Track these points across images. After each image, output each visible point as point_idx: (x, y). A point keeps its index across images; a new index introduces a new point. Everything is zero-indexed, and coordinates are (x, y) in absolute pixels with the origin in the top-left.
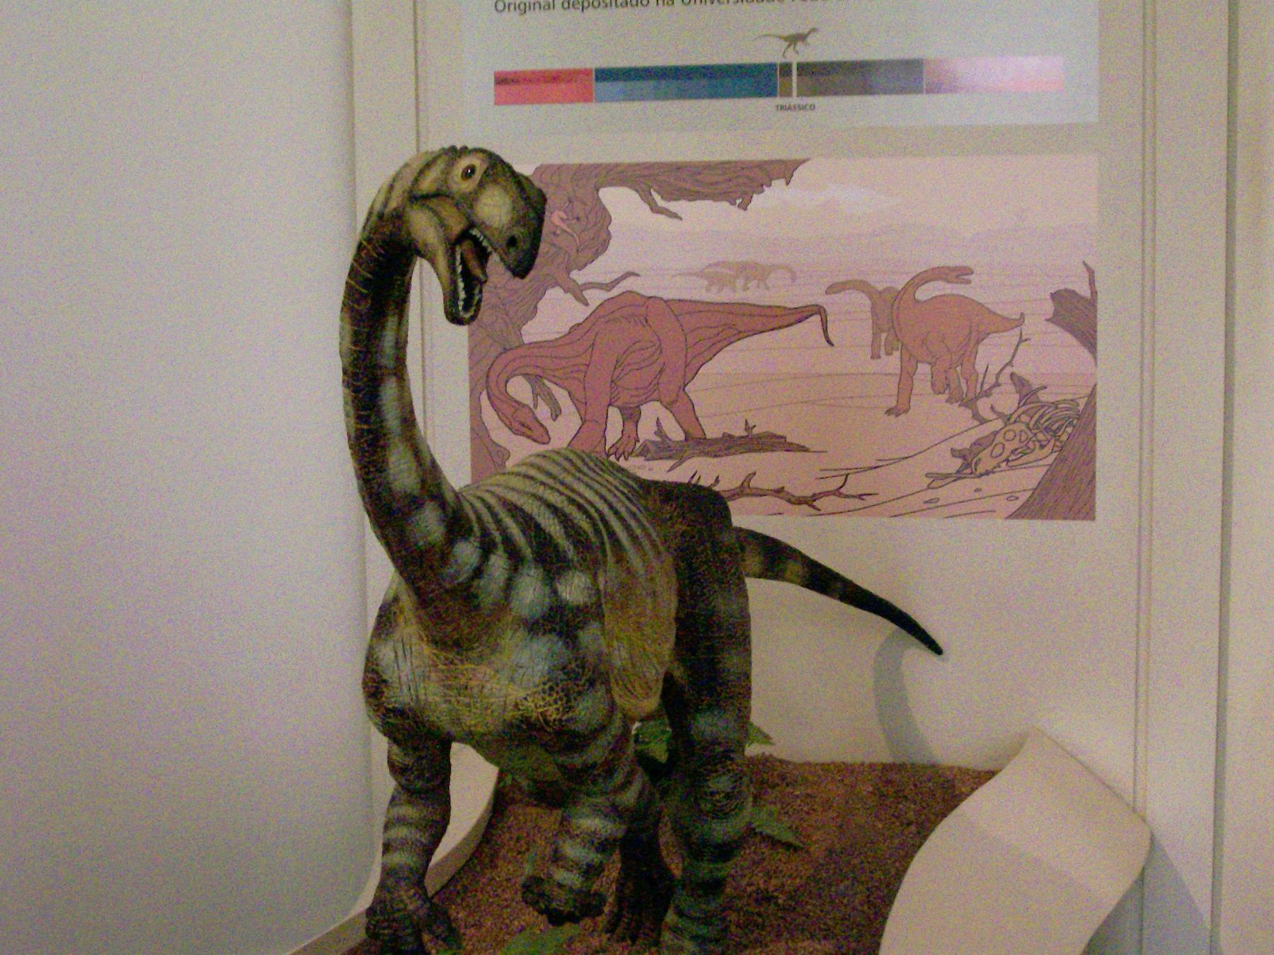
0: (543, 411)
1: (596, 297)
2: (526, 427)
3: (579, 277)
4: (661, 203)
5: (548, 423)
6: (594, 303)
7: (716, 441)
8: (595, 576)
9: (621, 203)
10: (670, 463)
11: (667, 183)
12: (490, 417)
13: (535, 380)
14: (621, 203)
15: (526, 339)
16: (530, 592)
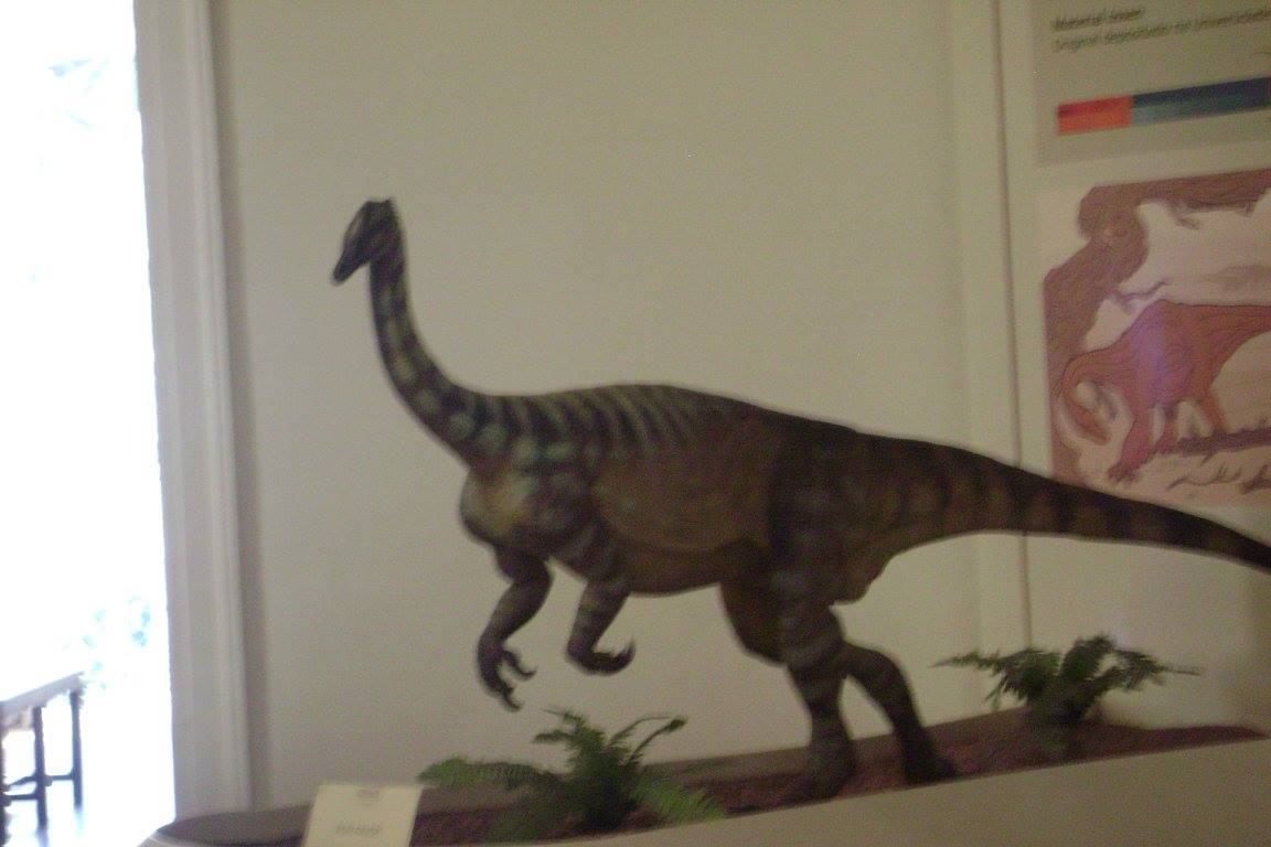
0: (1102, 413)
1: (1140, 305)
2: (1092, 429)
3: (1130, 285)
4: (1186, 216)
6: (1138, 311)
7: (1235, 435)
9: (1153, 214)
10: (1202, 458)
11: (1194, 194)
12: (1065, 423)
13: (1097, 382)
14: (1153, 214)
16: (525, 450)
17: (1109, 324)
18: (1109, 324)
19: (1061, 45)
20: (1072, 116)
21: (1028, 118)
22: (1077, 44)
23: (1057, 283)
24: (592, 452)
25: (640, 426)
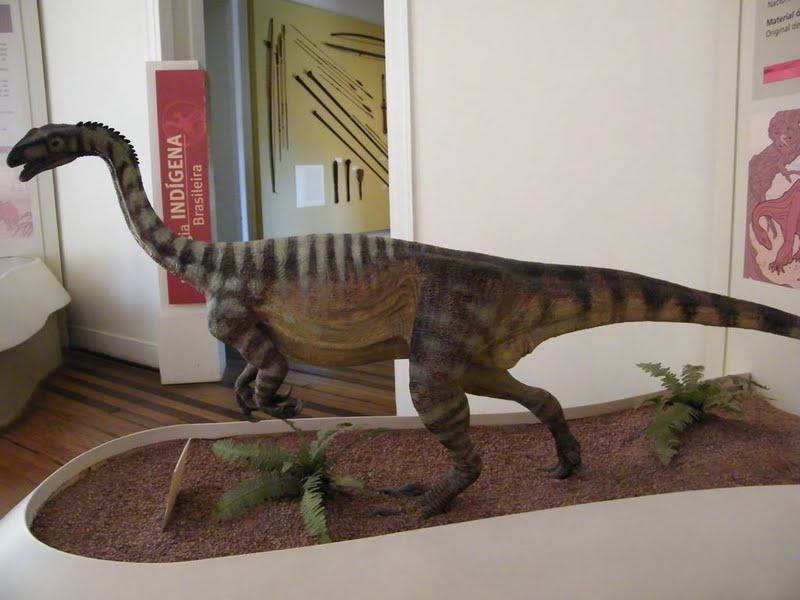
0: (770, 234)
1: (794, 178)
2: (766, 243)
3: (789, 168)
5: (772, 240)
8: (247, 282)
12: (752, 235)
13: (769, 218)
15: (768, 199)
17: (779, 187)
18: (779, 187)
19: (769, 34)
20: (771, 73)
21: (751, 72)
22: (777, 33)
23: (755, 163)
24: (255, 286)
25: (303, 267)
